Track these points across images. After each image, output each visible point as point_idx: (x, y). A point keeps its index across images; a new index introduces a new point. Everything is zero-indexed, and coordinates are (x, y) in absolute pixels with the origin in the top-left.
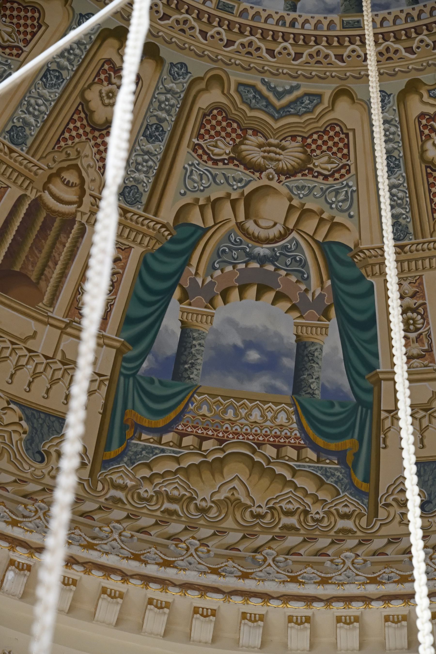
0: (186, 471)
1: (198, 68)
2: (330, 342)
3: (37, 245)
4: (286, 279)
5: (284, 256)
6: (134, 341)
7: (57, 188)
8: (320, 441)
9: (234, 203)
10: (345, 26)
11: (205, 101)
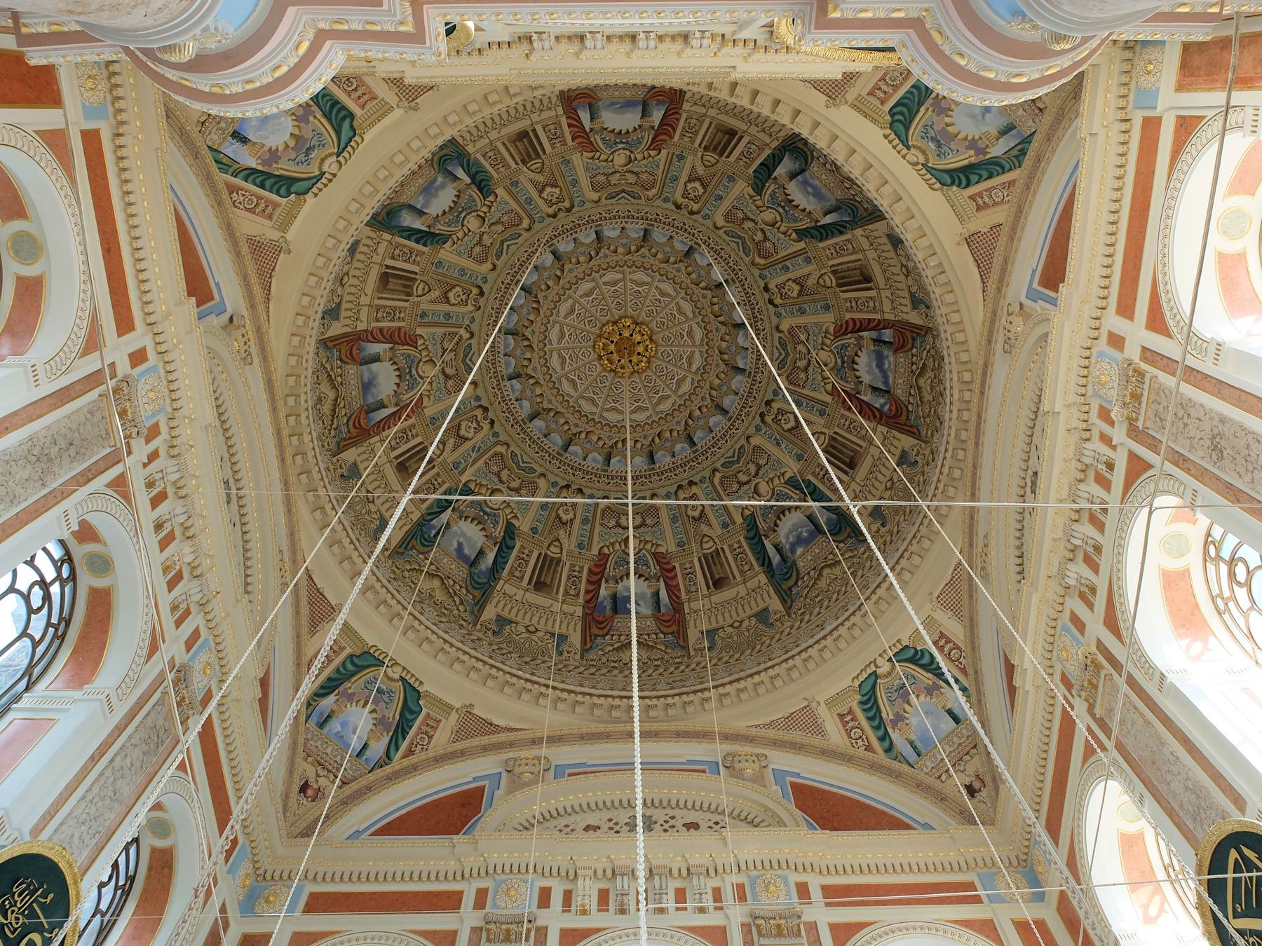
1: (756, 272)
2: (781, 171)
3: (850, 276)
5: (774, 203)
11: (762, 261)
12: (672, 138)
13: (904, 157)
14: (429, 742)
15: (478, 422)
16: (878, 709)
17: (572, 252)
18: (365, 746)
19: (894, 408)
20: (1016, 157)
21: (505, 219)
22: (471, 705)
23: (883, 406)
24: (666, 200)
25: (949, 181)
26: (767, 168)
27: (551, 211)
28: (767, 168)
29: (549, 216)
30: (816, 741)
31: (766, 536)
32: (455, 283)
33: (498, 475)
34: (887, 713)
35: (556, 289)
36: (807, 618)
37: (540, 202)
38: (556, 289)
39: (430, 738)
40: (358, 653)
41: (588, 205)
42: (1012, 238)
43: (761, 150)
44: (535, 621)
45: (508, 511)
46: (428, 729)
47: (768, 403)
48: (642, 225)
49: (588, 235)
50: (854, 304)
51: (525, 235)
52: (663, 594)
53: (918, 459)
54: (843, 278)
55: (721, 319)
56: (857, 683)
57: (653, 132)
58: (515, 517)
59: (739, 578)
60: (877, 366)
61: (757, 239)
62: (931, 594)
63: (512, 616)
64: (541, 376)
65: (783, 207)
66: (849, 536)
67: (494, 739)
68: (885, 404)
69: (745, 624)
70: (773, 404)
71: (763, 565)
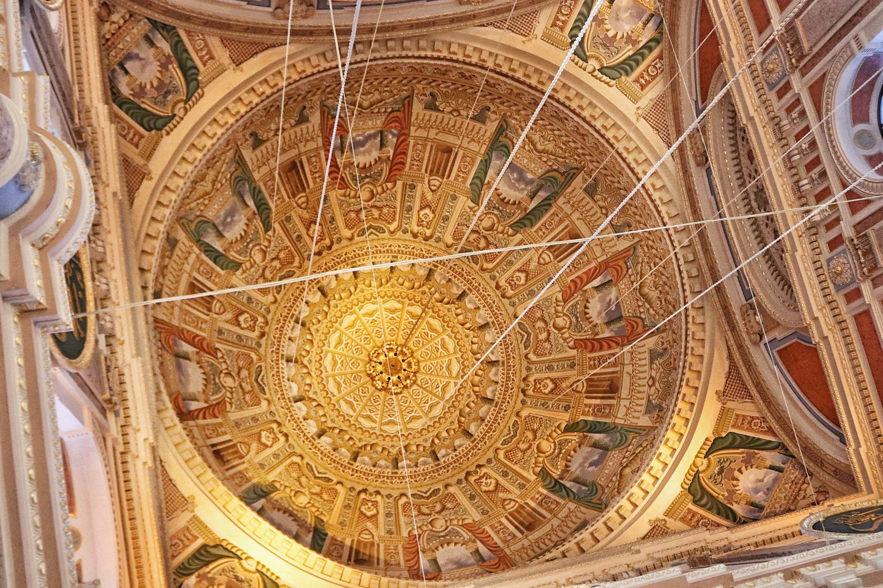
0: (219, 173)
2: (218, 245)
4: (239, 246)
6: (254, 188)
7: (303, 199)
8: (199, 219)
9: (267, 247)
10: (293, 315)
11: (297, 259)
12: (204, 339)
13: (182, 119)
14: (757, 418)
15: (481, 478)
16: (629, 58)
17: (317, 421)
18: (772, 468)
19: (393, 125)
20: (168, 32)
21: (295, 475)
22: (717, 393)
23: (394, 135)
24: (259, 345)
26: (216, 256)
27: (282, 439)
28: (216, 256)
29: (287, 440)
30: (668, 100)
31: (526, 209)
32: (357, 512)
33: (524, 452)
34: (628, 51)
35: (352, 432)
36: (580, 151)
37: (276, 447)
38: (352, 432)
39: (753, 418)
40: (690, 497)
41: (273, 409)
43: (202, 262)
44: (644, 382)
45: (555, 435)
46: (746, 422)
47: (415, 236)
48: (283, 364)
49: (300, 409)
50: (317, 175)
51: (306, 460)
52: (596, 282)
53: (428, 93)
54: (297, 187)
55: (352, 289)
56: (613, 82)
57: (201, 353)
58: (558, 427)
59: (566, 223)
60: (363, 146)
61: (279, 266)
62: (524, 42)
63: (644, 402)
64: (431, 435)
65: (248, 244)
66: (506, 136)
67: (740, 363)
68: (392, 133)
69: (601, 203)
70: (415, 231)
71: (550, 205)
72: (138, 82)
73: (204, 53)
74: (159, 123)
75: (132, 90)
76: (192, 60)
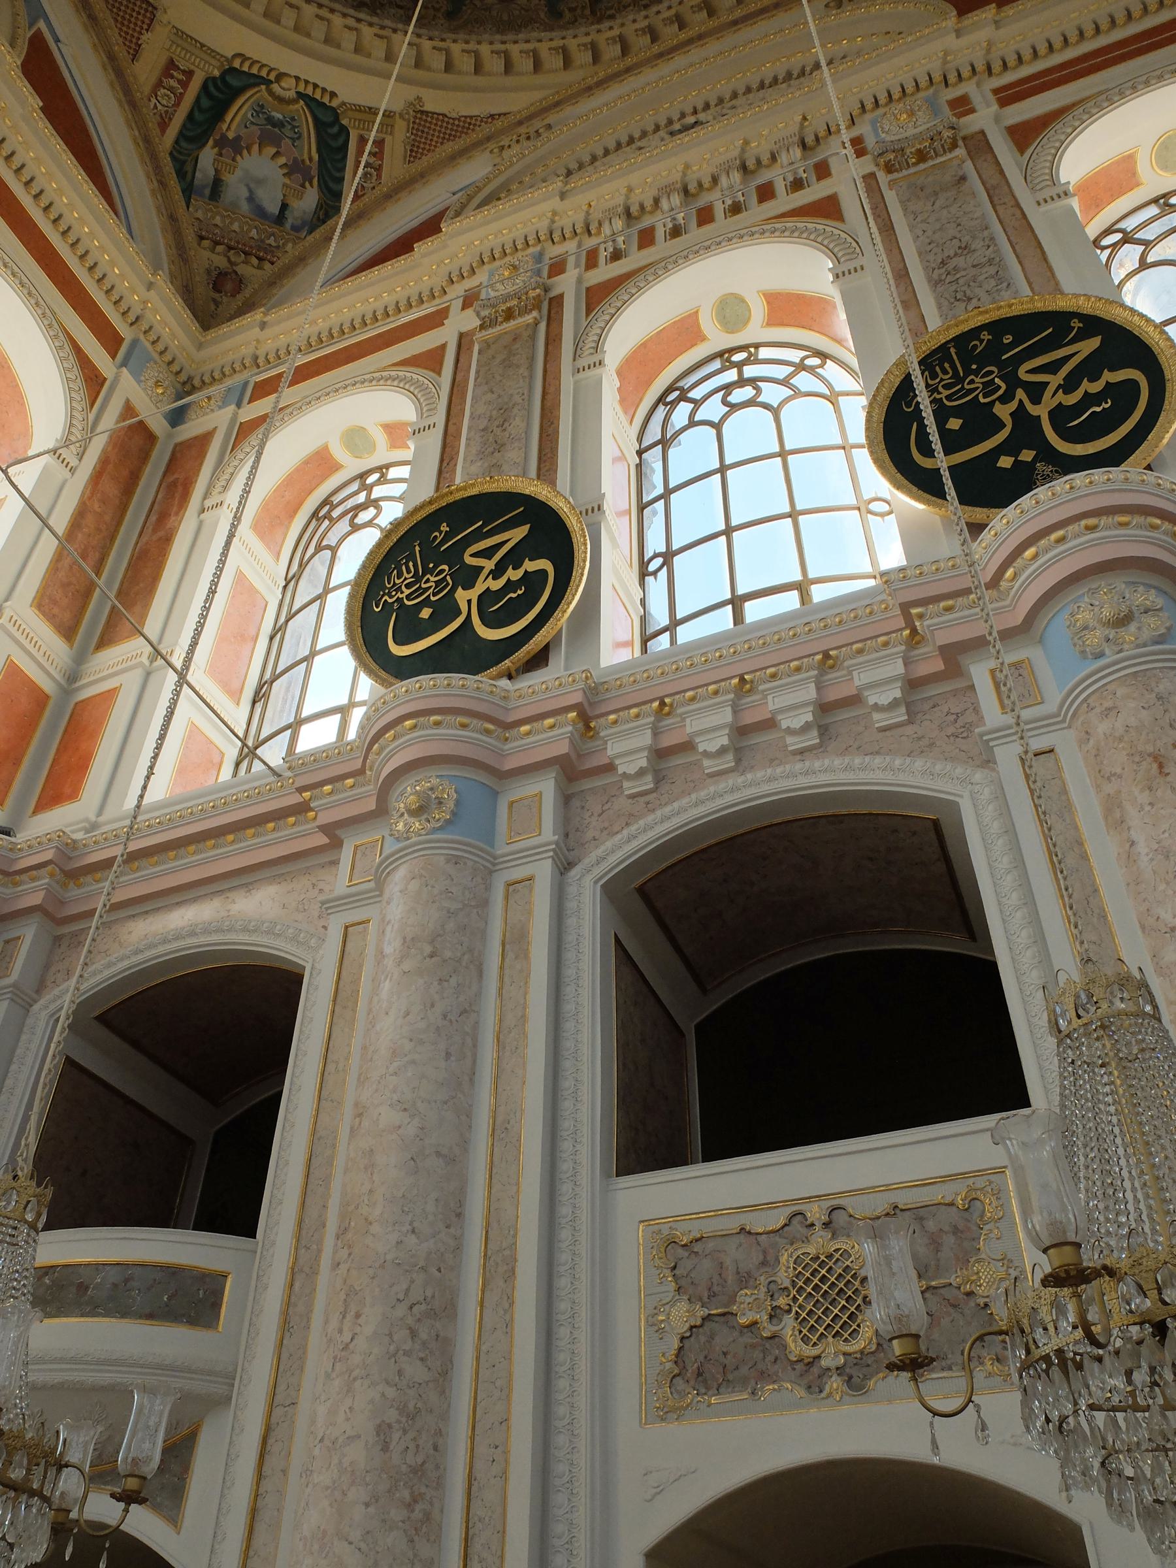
13: (297, 78)
20: (184, 162)
25: (228, 78)
42: (112, 57)
72: (288, 181)
73: (173, 83)
74: (327, 118)
75: (303, 186)
76: (198, 100)
